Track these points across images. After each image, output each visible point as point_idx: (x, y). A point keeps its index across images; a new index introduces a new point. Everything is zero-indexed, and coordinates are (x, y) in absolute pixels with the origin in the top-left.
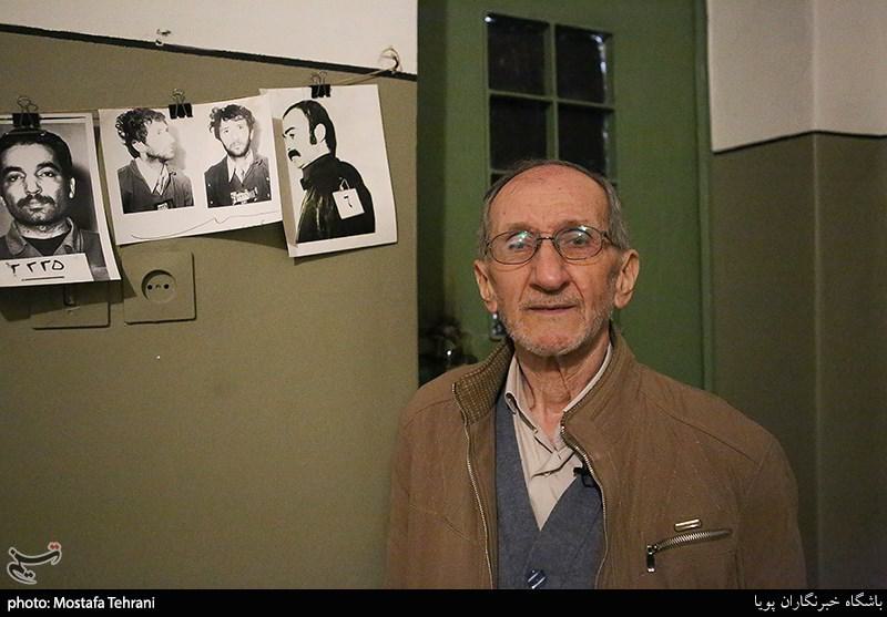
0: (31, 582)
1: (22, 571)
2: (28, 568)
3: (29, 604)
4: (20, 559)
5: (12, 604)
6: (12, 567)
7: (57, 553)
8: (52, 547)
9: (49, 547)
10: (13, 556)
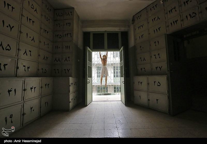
0: (8, 136)
1: (5, 133)
2: (7, 133)
3: (9, 141)
4: (5, 130)
6: (3, 132)
8: (12, 128)
9: (12, 128)
10: (3, 130)
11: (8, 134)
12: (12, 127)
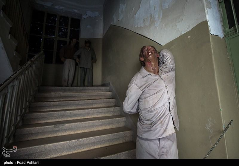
0: (9, 156)
1: (6, 154)
2: (7, 152)
3: (9, 163)
5: (5, 163)
6: (4, 153)
7: (16, 149)
8: (14, 147)
9: (13, 147)
10: (4, 150)
11: (10, 155)
12: (14, 146)
